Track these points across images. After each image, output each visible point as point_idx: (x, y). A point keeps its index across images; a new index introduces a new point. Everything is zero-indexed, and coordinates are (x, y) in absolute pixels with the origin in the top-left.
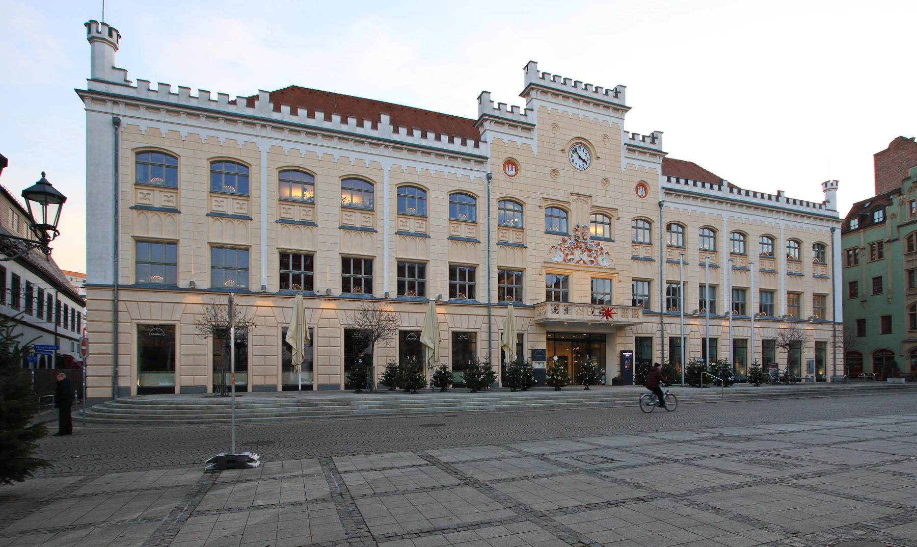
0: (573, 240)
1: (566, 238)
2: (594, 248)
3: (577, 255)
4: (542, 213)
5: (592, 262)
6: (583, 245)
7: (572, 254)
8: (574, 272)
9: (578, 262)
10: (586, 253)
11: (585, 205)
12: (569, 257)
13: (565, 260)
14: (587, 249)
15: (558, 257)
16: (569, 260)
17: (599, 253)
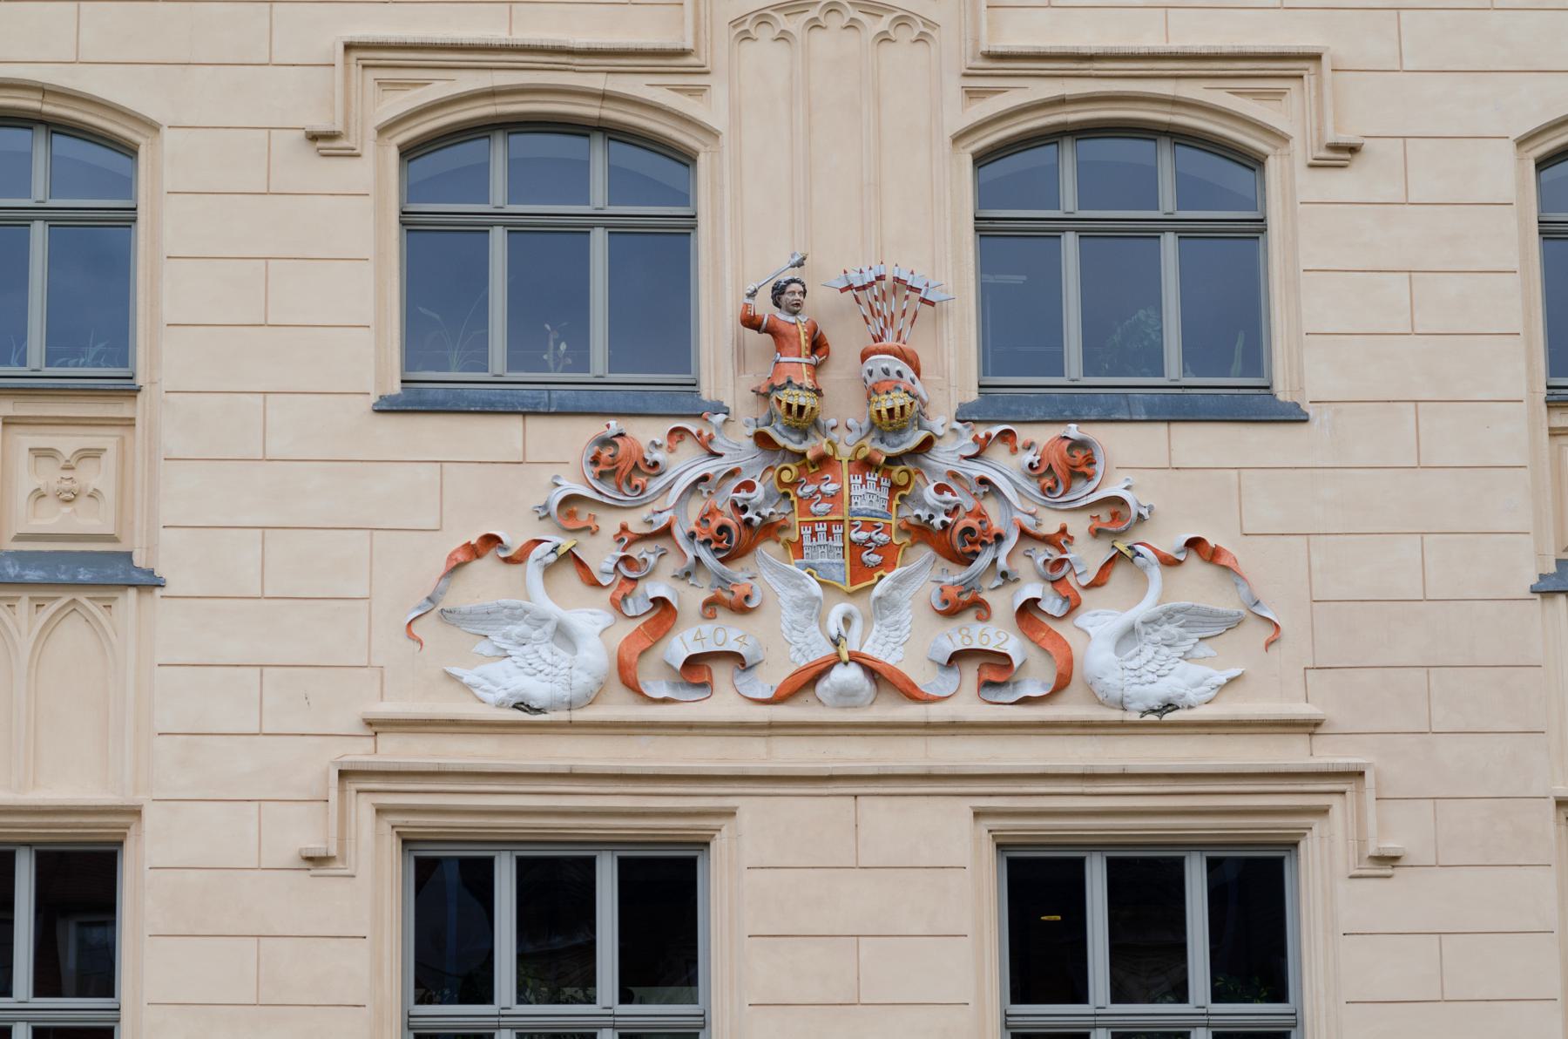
0: (737, 446)
1: (647, 434)
2: (1018, 503)
3: (790, 613)
4: (359, 214)
5: (995, 669)
6: (866, 495)
7: (741, 608)
8: (751, 809)
9: (808, 681)
10: (921, 577)
11: (903, 54)
12: (680, 645)
13: (627, 677)
14: (921, 532)
15: (561, 645)
16: (696, 668)
17: (1087, 556)
